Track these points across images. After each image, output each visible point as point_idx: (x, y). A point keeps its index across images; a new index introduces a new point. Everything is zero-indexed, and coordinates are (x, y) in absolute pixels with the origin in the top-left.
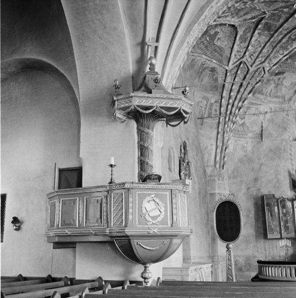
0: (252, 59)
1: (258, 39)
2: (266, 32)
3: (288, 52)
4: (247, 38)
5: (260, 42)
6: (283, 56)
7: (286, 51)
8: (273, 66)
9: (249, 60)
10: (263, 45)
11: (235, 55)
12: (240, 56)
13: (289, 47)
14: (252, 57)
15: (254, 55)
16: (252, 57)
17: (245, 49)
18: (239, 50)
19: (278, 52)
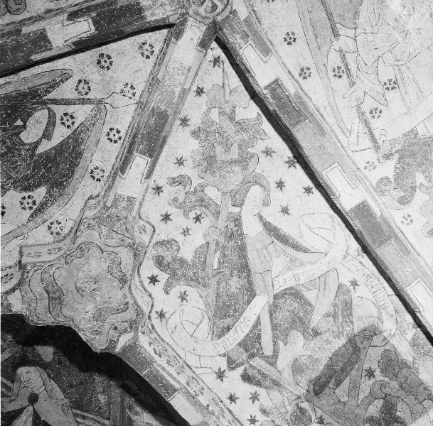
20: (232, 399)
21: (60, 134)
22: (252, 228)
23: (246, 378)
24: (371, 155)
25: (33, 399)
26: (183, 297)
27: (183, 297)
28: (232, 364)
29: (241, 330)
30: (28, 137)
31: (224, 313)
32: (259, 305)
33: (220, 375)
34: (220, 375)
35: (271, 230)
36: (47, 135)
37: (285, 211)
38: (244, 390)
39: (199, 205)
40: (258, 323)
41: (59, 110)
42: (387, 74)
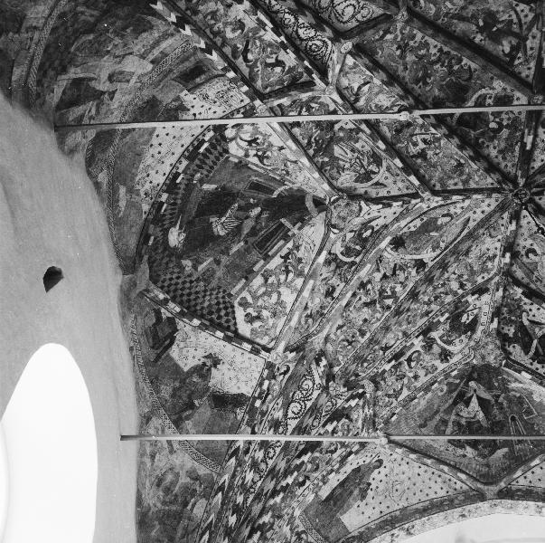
20: (537, 369)
21: (471, 318)
22: (526, 323)
23: (538, 363)
25: (475, 391)
26: (514, 347)
27: (514, 347)
28: (533, 360)
29: (533, 350)
30: (463, 321)
31: (526, 349)
32: (535, 342)
33: (531, 364)
34: (531, 364)
35: (531, 322)
36: (468, 319)
37: (534, 316)
38: (539, 366)
40: (536, 348)
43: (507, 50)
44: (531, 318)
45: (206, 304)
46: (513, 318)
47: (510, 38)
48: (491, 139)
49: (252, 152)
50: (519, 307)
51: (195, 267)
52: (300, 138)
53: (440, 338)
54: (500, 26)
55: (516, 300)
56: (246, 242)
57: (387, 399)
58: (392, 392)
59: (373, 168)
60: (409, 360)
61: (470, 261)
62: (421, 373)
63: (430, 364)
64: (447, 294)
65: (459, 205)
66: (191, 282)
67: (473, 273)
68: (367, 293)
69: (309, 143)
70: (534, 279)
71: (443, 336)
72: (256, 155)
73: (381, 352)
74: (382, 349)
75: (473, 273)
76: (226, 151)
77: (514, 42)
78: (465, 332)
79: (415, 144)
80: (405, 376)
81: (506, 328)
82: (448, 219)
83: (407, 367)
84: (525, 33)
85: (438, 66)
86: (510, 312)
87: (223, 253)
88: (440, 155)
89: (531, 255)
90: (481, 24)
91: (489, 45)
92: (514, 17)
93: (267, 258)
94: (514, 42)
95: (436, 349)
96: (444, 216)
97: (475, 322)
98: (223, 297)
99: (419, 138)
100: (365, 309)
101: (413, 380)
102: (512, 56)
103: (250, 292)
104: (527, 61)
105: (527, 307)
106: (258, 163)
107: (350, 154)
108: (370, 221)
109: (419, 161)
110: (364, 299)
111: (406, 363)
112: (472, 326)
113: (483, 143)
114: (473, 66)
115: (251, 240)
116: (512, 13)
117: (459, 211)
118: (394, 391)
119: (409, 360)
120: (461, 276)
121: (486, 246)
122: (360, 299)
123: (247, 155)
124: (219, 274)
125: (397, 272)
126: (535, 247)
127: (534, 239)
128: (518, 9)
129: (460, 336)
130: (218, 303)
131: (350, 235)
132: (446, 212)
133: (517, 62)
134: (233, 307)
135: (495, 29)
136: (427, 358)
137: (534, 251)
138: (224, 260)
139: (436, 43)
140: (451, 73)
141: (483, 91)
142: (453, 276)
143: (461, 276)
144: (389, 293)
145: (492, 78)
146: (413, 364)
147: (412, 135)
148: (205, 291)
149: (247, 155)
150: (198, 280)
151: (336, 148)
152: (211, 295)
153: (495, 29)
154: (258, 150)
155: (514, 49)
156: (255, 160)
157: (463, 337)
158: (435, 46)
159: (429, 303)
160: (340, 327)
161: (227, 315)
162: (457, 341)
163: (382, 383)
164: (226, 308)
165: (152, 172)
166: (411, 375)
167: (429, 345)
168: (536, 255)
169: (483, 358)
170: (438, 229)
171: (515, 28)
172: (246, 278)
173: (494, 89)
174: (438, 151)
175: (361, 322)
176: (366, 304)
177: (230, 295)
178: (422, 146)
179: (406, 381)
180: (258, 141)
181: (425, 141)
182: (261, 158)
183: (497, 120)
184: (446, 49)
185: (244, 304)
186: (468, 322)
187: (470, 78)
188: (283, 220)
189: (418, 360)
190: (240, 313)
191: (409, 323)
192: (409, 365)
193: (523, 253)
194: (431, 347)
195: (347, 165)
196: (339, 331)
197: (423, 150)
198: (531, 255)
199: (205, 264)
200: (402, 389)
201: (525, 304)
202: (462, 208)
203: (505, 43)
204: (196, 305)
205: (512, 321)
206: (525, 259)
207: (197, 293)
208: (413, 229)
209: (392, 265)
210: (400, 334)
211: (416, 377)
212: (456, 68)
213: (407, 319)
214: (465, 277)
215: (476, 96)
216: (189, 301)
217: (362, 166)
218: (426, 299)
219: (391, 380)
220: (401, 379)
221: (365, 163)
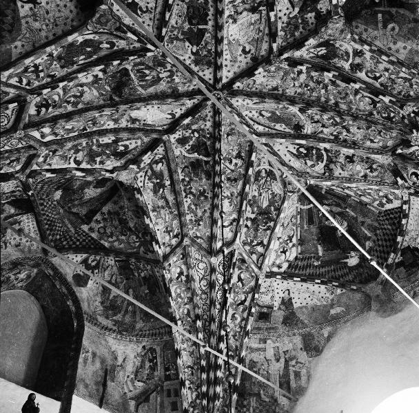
0: (39, 112)
1: (85, 88)
2: (108, 88)
3: (89, 167)
4: (73, 63)
5: (81, 96)
6: (76, 166)
7: (88, 163)
8: (47, 171)
9: (32, 110)
10: (80, 106)
11: (26, 70)
12: (28, 84)
13: (98, 159)
14: (44, 110)
15: (50, 109)
16: (44, 110)
17: (49, 80)
18: (41, 68)
19: (77, 151)
21: (319, 49)
24: (263, 12)
35: (293, 7)
39: (305, 22)
41: (316, 53)
42: (252, 27)
43: (160, 164)
44: (291, 9)
45: (390, 227)
46: (300, 21)
47: (155, 169)
48: (203, 130)
49: (291, 245)
50: (288, 23)
51: (369, 239)
52: (268, 237)
53: (347, 61)
54: (155, 181)
55: (285, 31)
56: (346, 208)
57: (414, 86)
58: (407, 84)
59: (263, 174)
60: (376, 78)
61: (279, 82)
62: (381, 67)
63: (371, 61)
64: (312, 77)
65: (250, 115)
66: (378, 240)
67: (286, 73)
68: (340, 133)
69: (268, 229)
70: (261, 34)
71: (345, 60)
72: (291, 242)
73: (378, 105)
74: (375, 107)
75: (286, 73)
76: (296, 258)
77: (154, 166)
78: (333, 45)
79: (236, 164)
80: (390, 78)
81: (310, 21)
82: (263, 113)
83: (382, 79)
84: (147, 167)
85: (193, 190)
86: (297, 28)
87: (357, 221)
88: (231, 148)
89: (247, 50)
90: (162, 190)
91: (166, 173)
92: (146, 181)
93: (350, 196)
94: (154, 166)
95: (358, 60)
96: (263, 116)
97: (320, 45)
98: (382, 216)
99: (232, 167)
100: (351, 130)
101: (390, 71)
102: (160, 161)
103: (373, 202)
104: (156, 154)
105: (285, 19)
106: (295, 236)
107: (264, 195)
108: (294, 155)
109: (243, 154)
110: (345, 133)
111: (379, 80)
112: (326, 44)
113: (208, 134)
114: (180, 171)
115: (343, 206)
116: (146, 184)
117: (254, 112)
118: (405, 82)
119: (376, 78)
120: (294, 79)
121: (263, 80)
122: (346, 135)
123: (294, 245)
124: (369, 221)
125: (316, 120)
126: (240, 52)
127: (236, 58)
128: (142, 184)
129: (337, 48)
130: (387, 219)
131: (310, 163)
132: (261, 117)
133: (161, 156)
134: (386, 211)
135: (158, 181)
136: (368, 65)
137: (244, 51)
138: (360, 219)
139: (185, 203)
140: (191, 180)
141: (186, 155)
142: (297, 84)
143: (294, 79)
144: (332, 120)
145: (177, 157)
146: (378, 75)
147: (233, 171)
148: (382, 229)
149: (294, 245)
150: (376, 235)
151: (264, 206)
152: (383, 225)
153: (158, 181)
154: (287, 245)
155: (157, 162)
156: (294, 240)
157: (337, 45)
158: (187, 201)
159: (325, 87)
160: (372, 141)
161: (392, 213)
162: (343, 48)
163: (403, 93)
164: (389, 214)
165: (321, 295)
166: (387, 74)
167: (357, 67)
168: (244, 48)
169: (342, 31)
170: (273, 113)
171: (150, 173)
172: (366, 205)
173: (181, 152)
174: (231, 151)
175: (361, 130)
176: (348, 131)
177: (379, 213)
178: (234, 161)
179: (393, 77)
180: (282, 250)
181: (231, 162)
182: (290, 238)
183: (192, 135)
184: (184, 194)
185: (382, 205)
186: (323, 48)
187: (185, 167)
188: (323, 193)
189: (372, 71)
190: (388, 206)
191: (347, 94)
192: (379, 77)
193: (249, 55)
194: (358, 65)
195: (270, 192)
196: (375, 141)
197: (236, 158)
198: (247, 50)
199: (366, 232)
200: (402, 78)
201: (283, 23)
202: (250, 112)
203: (159, 169)
204: (391, 234)
205: (303, 20)
206: (253, 51)
207: (384, 235)
208: (284, 126)
209: (314, 124)
210: (358, 97)
211: (387, 70)
212: (187, 179)
213: (344, 98)
214: (292, 75)
215: (191, 156)
216: (389, 240)
217: (266, 181)
218: (323, 91)
219: (398, 88)
220: (393, 80)
221: (264, 180)
